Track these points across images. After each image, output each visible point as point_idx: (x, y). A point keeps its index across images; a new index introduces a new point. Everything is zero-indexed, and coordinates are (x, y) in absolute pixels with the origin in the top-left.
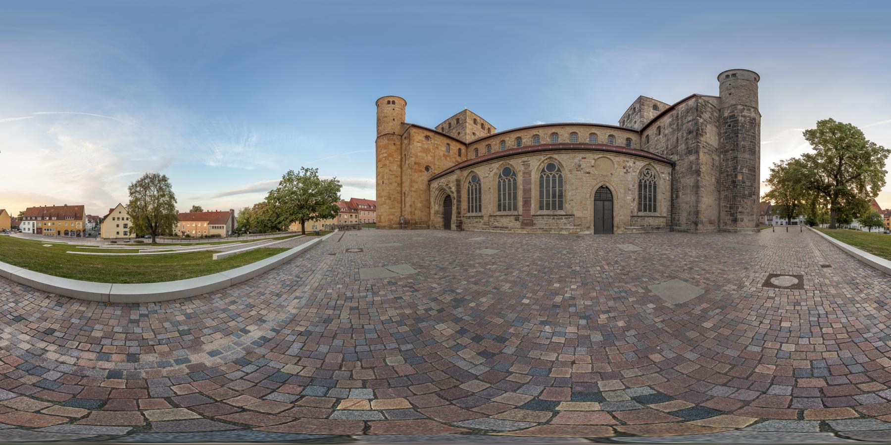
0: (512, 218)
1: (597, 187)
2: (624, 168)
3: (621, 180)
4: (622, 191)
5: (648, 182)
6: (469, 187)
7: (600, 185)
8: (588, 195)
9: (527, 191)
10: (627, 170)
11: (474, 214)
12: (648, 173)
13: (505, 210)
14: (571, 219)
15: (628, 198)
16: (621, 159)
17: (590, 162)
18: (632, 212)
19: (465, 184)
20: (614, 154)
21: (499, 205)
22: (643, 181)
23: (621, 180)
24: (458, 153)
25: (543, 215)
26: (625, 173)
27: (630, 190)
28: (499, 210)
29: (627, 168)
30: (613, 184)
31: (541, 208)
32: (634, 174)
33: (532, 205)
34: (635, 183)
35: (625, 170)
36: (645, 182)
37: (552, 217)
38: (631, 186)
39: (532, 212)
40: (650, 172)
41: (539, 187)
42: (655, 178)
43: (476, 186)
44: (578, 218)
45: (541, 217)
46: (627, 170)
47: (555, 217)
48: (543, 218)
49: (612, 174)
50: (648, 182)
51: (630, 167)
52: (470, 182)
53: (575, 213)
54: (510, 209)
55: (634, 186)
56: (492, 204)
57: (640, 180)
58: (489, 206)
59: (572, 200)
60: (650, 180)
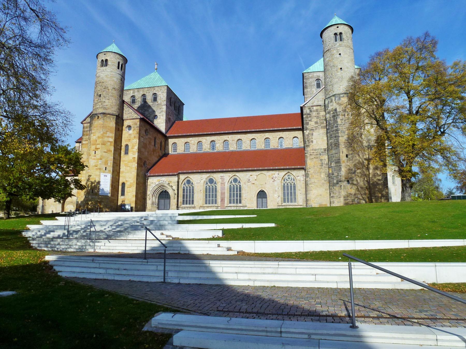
2: (272, 179)
5: (289, 184)
6: (184, 187)
8: (254, 196)
9: (223, 194)
10: (274, 180)
12: (289, 178)
13: (209, 203)
15: (275, 195)
16: (271, 172)
20: (266, 171)
21: (206, 201)
22: (286, 184)
23: (271, 186)
25: (231, 206)
26: (273, 181)
27: (276, 191)
28: (206, 203)
29: (274, 178)
30: (267, 189)
31: (230, 203)
32: (279, 181)
33: (226, 201)
34: (279, 186)
35: (273, 180)
36: (288, 184)
38: (277, 189)
39: (226, 205)
40: (290, 177)
41: (229, 192)
42: (294, 180)
43: (190, 187)
46: (274, 180)
49: (266, 183)
50: (289, 184)
51: (276, 177)
52: (185, 184)
54: (212, 203)
56: (202, 200)
59: (246, 199)
60: (291, 182)
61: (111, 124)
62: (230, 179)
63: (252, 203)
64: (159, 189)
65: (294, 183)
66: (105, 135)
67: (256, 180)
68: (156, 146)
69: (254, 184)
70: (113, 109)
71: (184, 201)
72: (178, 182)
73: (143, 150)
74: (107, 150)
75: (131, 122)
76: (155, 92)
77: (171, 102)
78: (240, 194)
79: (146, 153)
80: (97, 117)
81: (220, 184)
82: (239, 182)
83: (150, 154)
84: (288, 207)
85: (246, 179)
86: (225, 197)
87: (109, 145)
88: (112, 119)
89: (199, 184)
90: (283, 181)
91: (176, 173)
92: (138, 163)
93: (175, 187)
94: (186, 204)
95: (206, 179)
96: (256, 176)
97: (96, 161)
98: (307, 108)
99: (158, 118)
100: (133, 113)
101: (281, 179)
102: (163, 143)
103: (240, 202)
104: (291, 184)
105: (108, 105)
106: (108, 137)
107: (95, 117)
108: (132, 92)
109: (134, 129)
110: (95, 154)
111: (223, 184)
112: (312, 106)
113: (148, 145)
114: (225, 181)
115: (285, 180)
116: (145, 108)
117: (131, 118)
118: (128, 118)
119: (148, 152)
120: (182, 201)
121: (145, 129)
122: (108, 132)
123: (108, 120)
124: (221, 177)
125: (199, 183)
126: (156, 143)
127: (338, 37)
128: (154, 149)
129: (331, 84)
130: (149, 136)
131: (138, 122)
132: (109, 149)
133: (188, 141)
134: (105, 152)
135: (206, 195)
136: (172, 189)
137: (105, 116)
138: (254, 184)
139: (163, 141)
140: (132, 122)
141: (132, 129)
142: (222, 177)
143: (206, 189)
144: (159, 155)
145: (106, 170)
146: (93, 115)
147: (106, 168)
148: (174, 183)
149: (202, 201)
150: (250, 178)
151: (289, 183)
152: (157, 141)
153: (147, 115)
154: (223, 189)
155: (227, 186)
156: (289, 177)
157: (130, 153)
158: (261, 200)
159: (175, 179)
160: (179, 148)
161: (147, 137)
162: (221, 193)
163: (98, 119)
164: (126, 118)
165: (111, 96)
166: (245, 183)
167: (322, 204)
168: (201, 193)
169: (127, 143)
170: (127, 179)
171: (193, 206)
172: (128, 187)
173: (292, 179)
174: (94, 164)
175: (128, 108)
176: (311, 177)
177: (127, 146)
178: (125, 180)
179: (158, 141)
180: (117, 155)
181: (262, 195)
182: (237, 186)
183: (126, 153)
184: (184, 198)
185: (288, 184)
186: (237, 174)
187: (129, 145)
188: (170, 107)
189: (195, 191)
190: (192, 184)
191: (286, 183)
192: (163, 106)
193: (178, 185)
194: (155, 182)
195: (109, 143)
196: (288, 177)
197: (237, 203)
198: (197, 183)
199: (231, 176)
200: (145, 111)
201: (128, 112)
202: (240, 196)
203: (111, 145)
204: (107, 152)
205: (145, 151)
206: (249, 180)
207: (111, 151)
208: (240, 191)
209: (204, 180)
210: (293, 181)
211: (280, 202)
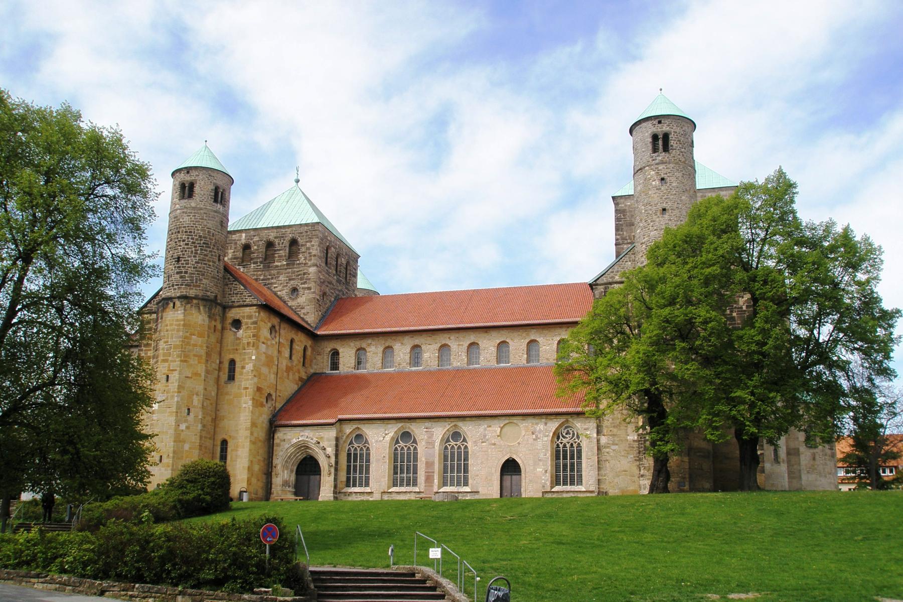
3: (530, 450)
5: (568, 446)
8: (493, 470)
10: (537, 436)
15: (538, 470)
17: (496, 431)
18: (544, 486)
19: (345, 444)
20: (521, 418)
22: (561, 446)
23: (530, 450)
26: (534, 440)
27: (540, 460)
28: (395, 485)
32: (546, 439)
33: (436, 481)
34: (547, 450)
38: (542, 456)
39: (435, 490)
40: (571, 432)
42: (578, 437)
43: (362, 449)
50: (568, 446)
51: (540, 431)
52: (351, 443)
53: (480, 490)
57: (558, 446)
58: (382, 480)
59: (477, 476)
60: (571, 441)
63: (490, 486)
64: (298, 453)
65: (579, 444)
67: (498, 436)
68: (294, 357)
69: (494, 444)
71: (348, 479)
72: (337, 439)
73: (265, 370)
77: (329, 255)
79: (273, 376)
80: (171, 305)
81: (423, 443)
82: (465, 440)
84: (565, 495)
86: (433, 472)
89: (380, 444)
90: (556, 440)
91: (333, 421)
92: (253, 399)
93: (330, 451)
94: (354, 485)
95: (396, 432)
98: (601, 287)
101: (551, 434)
102: (309, 352)
104: (572, 445)
107: (168, 304)
108: (244, 235)
109: (248, 327)
110: (167, 380)
111: (430, 444)
112: (611, 283)
114: (434, 438)
115: (561, 437)
117: (242, 303)
120: (344, 479)
121: (269, 325)
123: (194, 311)
125: (380, 441)
126: (294, 352)
127: (660, 142)
128: (290, 365)
129: (644, 241)
131: (255, 312)
133: (364, 345)
135: (395, 467)
136: (325, 453)
137: (188, 303)
138: (494, 444)
141: (244, 327)
143: (396, 455)
144: (301, 379)
145: (188, 414)
146: (163, 299)
148: (329, 440)
149: (387, 479)
151: (568, 443)
152: (297, 347)
156: (568, 431)
158: (510, 479)
159: (332, 433)
160: (343, 362)
161: (274, 342)
162: (427, 463)
163: (174, 307)
164: (230, 304)
167: (628, 489)
168: (385, 462)
169: (231, 356)
171: (368, 490)
173: (574, 434)
176: (607, 432)
177: (232, 362)
179: (298, 348)
181: (511, 467)
182: (459, 448)
183: (231, 377)
184: (348, 472)
185: (565, 446)
189: (373, 458)
190: (367, 442)
191: (561, 443)
192: (310, 267)
193: (337, 446)
194: (289, 437)
196: (566, 431)
198: (377, 441)
204: (191, 378)
205: (270, 372)
207: (200, 375)
208: (466, 459)
209: (391, 434)
210: (577, 440)
211: (548, 483)
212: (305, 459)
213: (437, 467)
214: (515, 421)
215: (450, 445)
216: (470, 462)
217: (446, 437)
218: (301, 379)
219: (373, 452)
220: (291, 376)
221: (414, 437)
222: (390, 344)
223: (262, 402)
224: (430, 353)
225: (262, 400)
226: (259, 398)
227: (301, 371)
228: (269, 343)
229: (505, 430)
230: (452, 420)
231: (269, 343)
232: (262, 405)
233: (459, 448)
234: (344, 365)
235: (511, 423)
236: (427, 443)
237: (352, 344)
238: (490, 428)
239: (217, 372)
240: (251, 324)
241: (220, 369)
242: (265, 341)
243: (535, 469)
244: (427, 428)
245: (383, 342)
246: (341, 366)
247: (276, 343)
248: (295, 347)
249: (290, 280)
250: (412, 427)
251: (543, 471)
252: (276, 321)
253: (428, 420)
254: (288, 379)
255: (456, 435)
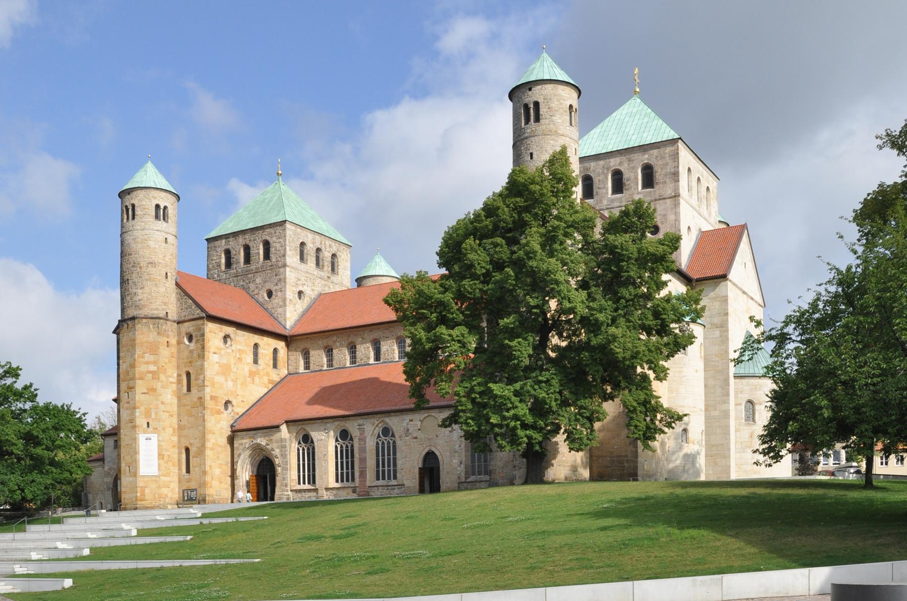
0: (350, 490)
1: (424, 453)
4: (448, 454)
7: (426, 450)
11: (310, 487)
14: (403, 489)
18: (459, 477)
20: (437, 410)
23: (447, 442)
24: (271, 362)
25: (378, 486)
27: (455, 452)
33: (368, 476)
37: (386, 488)
38: (457, 447)
39: (368, 484)
44: (408, 487)
45: (376, 488)
47: (389, 488)
48: (378, 489)
49: (437, 436)
53: (405, 482)
55: (460, 446)
59: (402, 469)
61: (151, 337)
62: (375, 429)
66: (141, 360)
67: (419, 430)
68: (260, 361)
69: (416, 438)
70: (154, 306)
74: (147, 389)
75: (191, 325)
76: (265, 237)
78: (395, 460)
79: (230, 384)
82: (393, 435)
83: (242, 384)
85: (402, 429)
86: (366, 468)
87: (151, 378)
88: (151, 326)
96: (420, 422)
97: (130, 412)
99: (273, 296)
100: (193, 307)
103: (395, 478)
105: (141, 300)
106: (147, 363)
111: (362, 440)
113: (232, 366)
114: (366, 434)
116: (249, 276)
118: (186, 319)
119: (235, 381)
122: (146, 353)
123: (145, 329)
124: (358, 427)
126: (260, 356)
130: (234, 347)
132: (151, 387)
134: (144, 393)
137: (139, 323)
138: (416, 438)
139: (279, 348)
140: (193, 326)
141: (194, 340)
142: (361, 427)
144: (270, 381)
145: (148, 427)
147: (148, 423)
150: (409, 426)
153: (254, 291)
154: (363, 450)
155: (371, 444)
157: (194, 390)
161: (230, 351)
165: (147, 280)
166: (400, 437)
169: (187, 369)
170: (192, 441)
172: (193, 457)
174: (128, 418)
175: (186, 297)
178: (188, 442)
180: (169, 396)
186: (387, 420)
187: (191, 372)
188: (302, 266)
190: (312, 442)
192: (280, 268)
195: (151, 375)
197: (389, 478)
199: (377, 423)
200: (250, 283)
201: (186, 306)
202: (395, 465)
203: (153, 378)
205: (226, 380)
206: (408, 430)
208: (395, 453)
211: (463, 475)
212: (263, 460)
213: (371, 462)
214: (433, 414)
215: (380, 440)
216: (398, 455)
217: (376, 432)
218: (270, 381)
219: (316, 450)
220: (257, 379)
221: (351, 436)
222: (353, 340)
223: (220, 410)
224: (366, 351)
225: (218, 407)
226: (214, 406)
227: (271, 373)
228: (223, 352)
229: (425, 422)
230: (379, 416)
231: (223, 352)
232: (219, 412)
233: (389, 443)
234: (314, 364)
235: (430, 416)
236: (359, 439)
237: (320, 343)
238: (411, 422)
239: (174, 386)
240: (201, 337)
241: (179, 382)
242: (217, 351)
243: (451, 461)
244: (359, 425)
245: (347, 338)
246: (311, 365)
247: (233, 351)
248: (260, 351)
249: (265, 282)
250: (346, 425)
251: (459, 463)
252: (230, 330)
253: (359, 418)
254: (254, 383)
255: (386, 431)
